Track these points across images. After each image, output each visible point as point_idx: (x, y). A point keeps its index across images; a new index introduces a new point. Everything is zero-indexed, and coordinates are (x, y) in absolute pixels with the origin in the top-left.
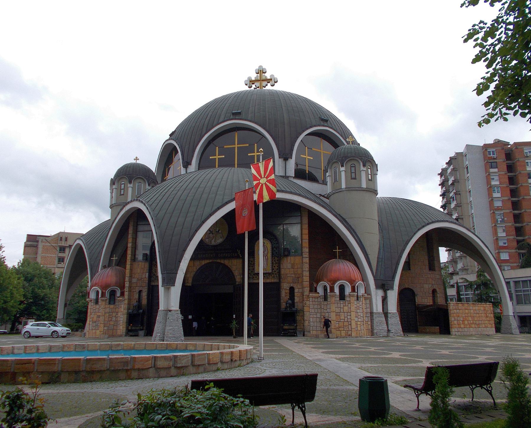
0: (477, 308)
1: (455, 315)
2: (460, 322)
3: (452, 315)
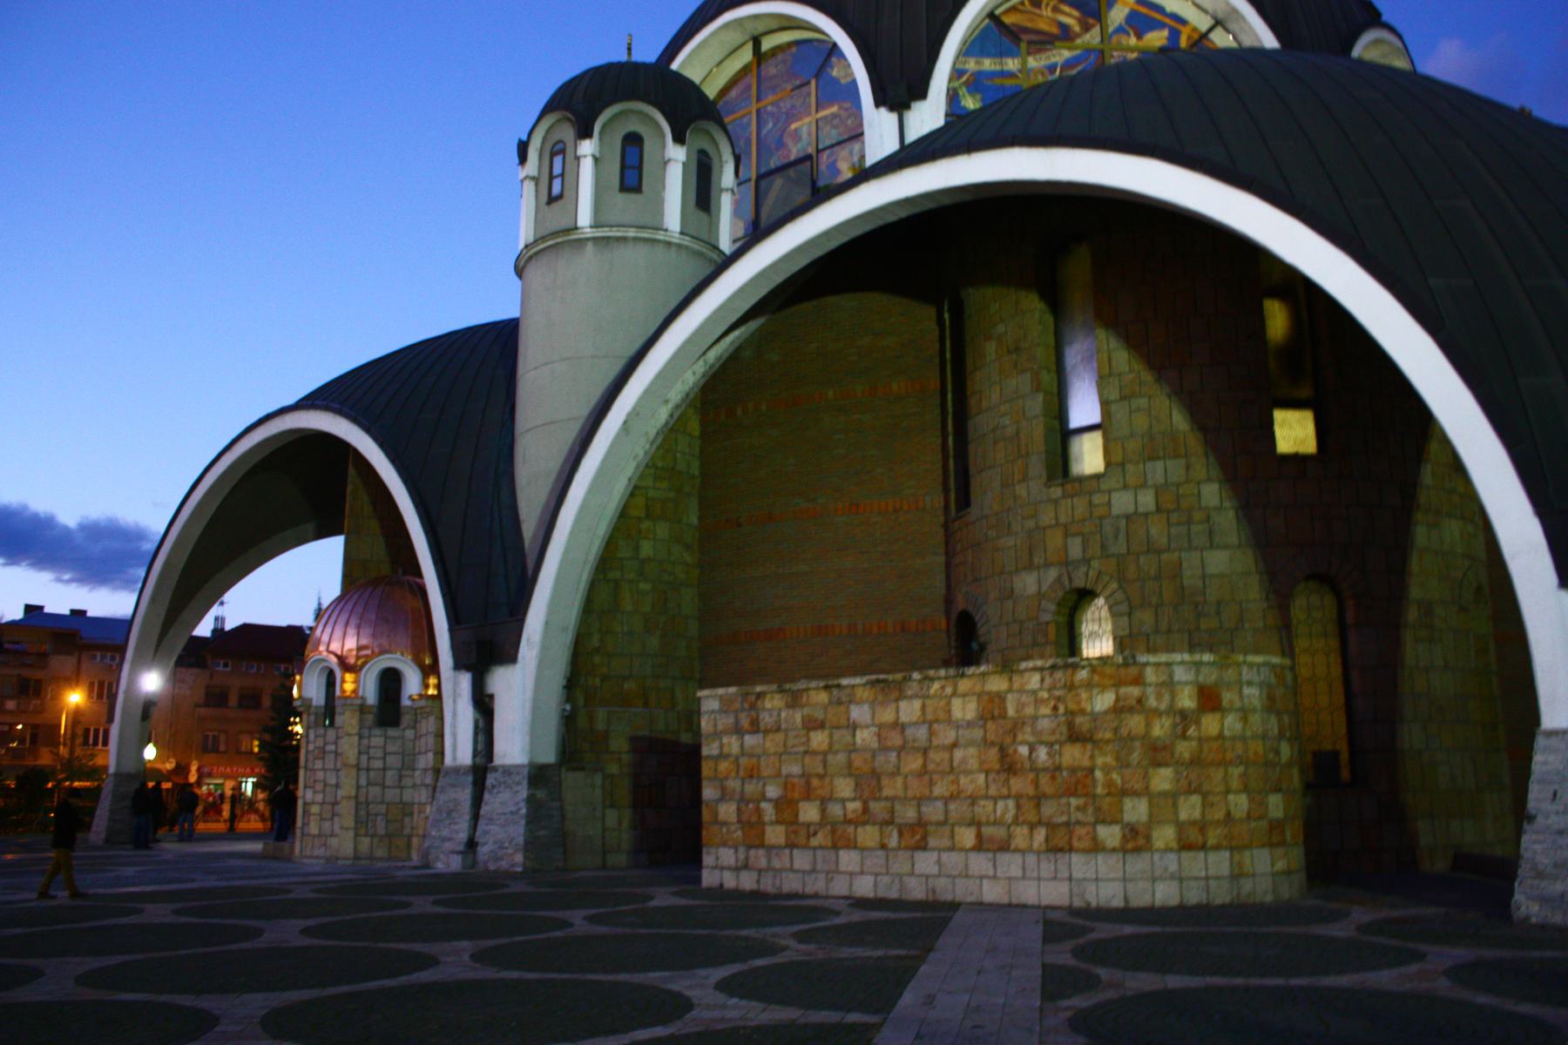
0: (909, 710)
1: (724, 766)
2: (758, 810)
3: (706, 770)
